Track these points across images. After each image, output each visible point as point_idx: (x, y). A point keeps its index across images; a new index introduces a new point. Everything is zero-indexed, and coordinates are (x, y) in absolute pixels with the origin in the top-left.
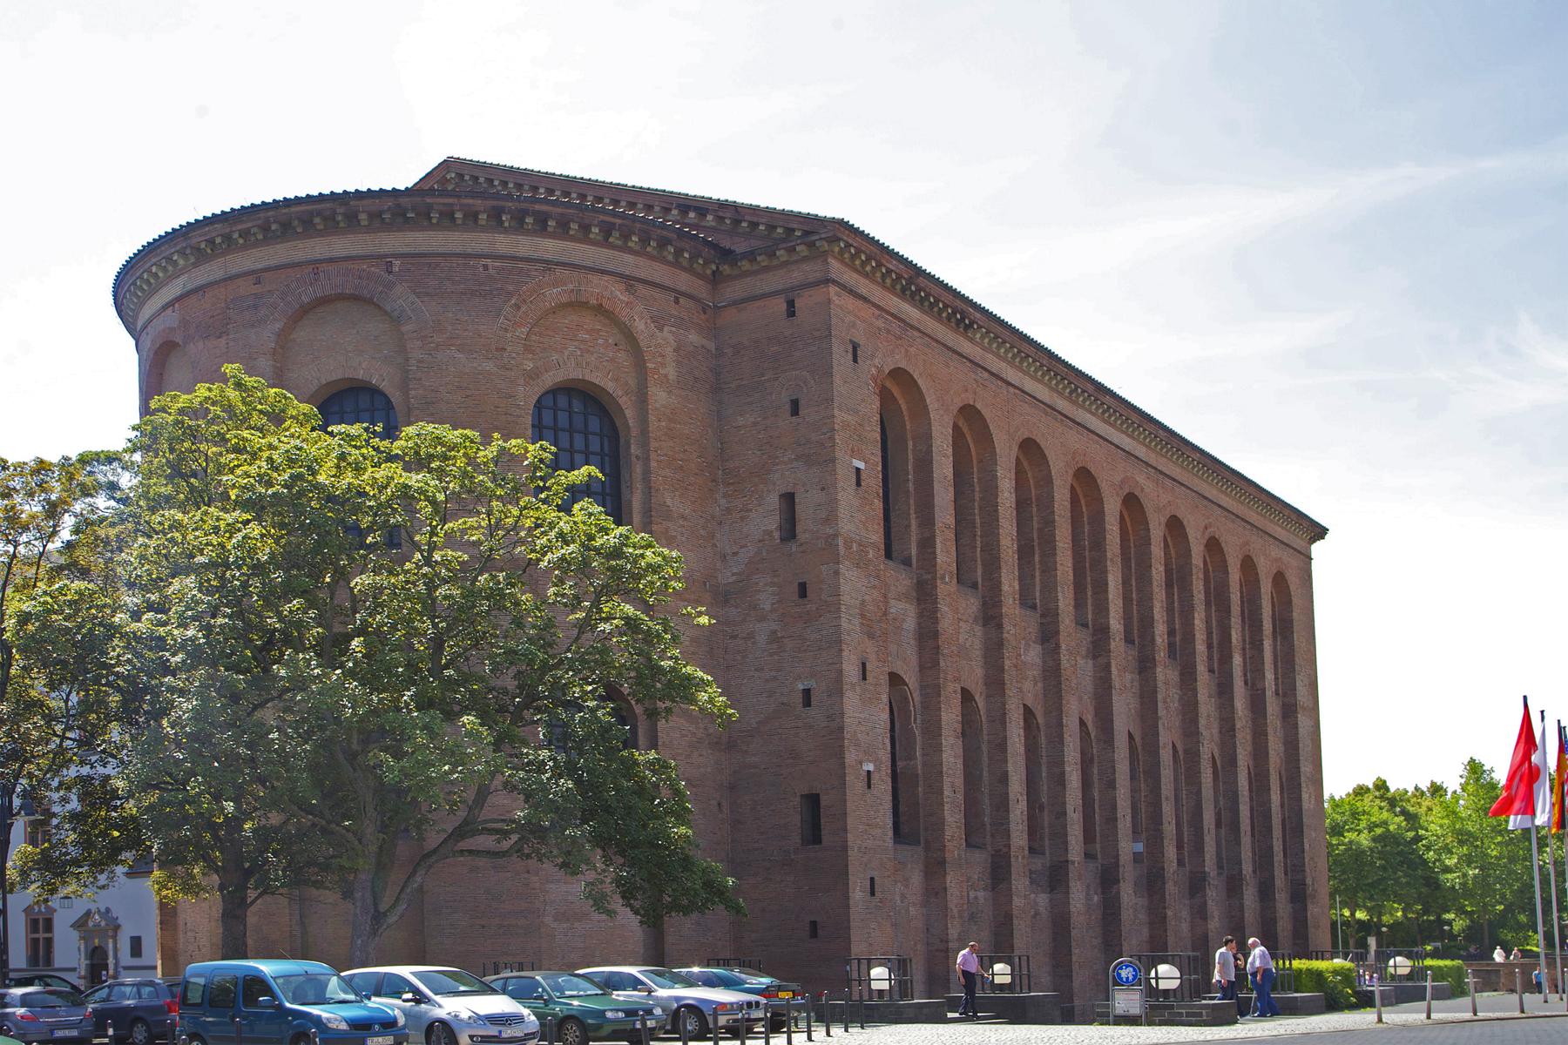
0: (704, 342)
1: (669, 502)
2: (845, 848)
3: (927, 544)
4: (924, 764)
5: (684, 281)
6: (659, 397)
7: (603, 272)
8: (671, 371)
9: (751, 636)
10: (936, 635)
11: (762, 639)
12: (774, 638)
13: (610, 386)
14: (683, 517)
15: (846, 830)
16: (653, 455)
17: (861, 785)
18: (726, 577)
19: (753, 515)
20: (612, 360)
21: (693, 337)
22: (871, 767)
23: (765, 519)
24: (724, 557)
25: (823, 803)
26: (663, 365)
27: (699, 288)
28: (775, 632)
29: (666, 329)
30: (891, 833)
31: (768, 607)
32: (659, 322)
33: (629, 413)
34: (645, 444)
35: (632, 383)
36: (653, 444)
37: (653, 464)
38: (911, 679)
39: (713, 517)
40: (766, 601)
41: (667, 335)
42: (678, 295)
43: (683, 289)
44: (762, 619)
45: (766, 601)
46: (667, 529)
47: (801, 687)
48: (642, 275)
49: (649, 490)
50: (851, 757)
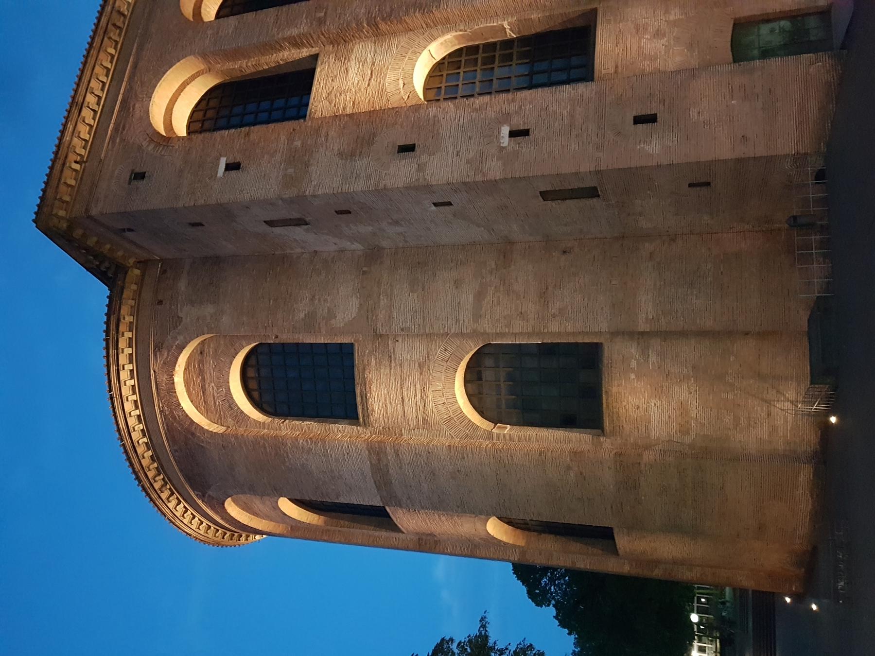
1: (302, 315)
2: (598, 172)
11: (399, 229)
12: (396, 223)
14: (312, 299)
15: (576, 174)
17: (524, 145)
22: (505, 130)
23: (298, 232)
25: (549, 188)
29: (180, 315)
30: (582, 88)
31: (370, 228)
40: (365, 229)
47: (434, 208)
50: (494, 170)
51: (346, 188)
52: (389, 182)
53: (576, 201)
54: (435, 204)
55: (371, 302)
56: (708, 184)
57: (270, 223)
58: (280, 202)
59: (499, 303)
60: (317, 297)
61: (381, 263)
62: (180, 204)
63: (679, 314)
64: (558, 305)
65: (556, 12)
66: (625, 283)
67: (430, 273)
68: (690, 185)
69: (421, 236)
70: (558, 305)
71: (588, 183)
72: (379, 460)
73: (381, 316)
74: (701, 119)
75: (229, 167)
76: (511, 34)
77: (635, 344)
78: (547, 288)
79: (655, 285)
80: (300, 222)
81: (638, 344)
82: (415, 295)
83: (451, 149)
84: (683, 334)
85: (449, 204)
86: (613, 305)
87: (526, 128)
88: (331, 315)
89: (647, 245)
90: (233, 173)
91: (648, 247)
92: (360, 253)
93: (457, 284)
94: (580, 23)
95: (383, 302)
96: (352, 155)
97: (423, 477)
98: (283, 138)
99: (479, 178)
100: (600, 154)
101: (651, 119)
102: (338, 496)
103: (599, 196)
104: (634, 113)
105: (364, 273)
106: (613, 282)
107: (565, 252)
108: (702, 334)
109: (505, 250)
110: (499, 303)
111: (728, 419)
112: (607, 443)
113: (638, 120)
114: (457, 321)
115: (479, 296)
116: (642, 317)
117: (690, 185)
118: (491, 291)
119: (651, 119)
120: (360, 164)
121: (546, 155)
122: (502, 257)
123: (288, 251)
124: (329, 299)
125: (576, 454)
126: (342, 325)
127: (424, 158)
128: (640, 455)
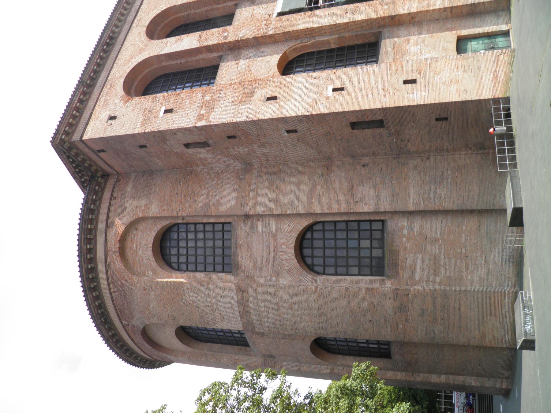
0: (131, 181)
2: (384, 109)
3: (209, 49)
4: (332, 34)
5: (107, 195)
6: (154, 210)
8: (143, 202)
9: (264, 154)
10: (256, 39)
11: (264, 150)
12: (263, 145)
13: (154, 234)
14: (208, 195)
16: (180, 214)
18: (238, 165)
19: (202, 157)
20: (143, 232)
22: (330, 88)
23: (202, 153)
24: (228, 166)
25: (355, 120)
26: (141, 207)
28: (259, 146)
29: (126, 205)
30: (372, 68)
31: (246, 150)
32: (124, 209)
33: (165, 223)
34: (177, 217)
35: (150, 222)
36: (175, 214)
37: (184, 214)
38: (284, 48)
39: (209, 173)
40: (244, 150)
41: (129, 204)
42: (112, 197)
43: (110, 194)
44: (253, 151)
45: (244, 150)
46: (214, 206)
47: (286, 134)
48: (105, 218)
49: (198, 216)
50: (323, 108)
51: (235, 120)
52: (261, 117)
53: (371, 130)
54: (288, 132)
55: (244, 196)
56: (446, 119)
57: (187, 146)
58: (195, 130)
59: (323, 195)
60: (211, 194)
61: (252, 173)
62: (136, 132)
63: (432, 200)
64: (359, 196)
65: (359, 33)
66: (400, 183)
67: (281, 178)
68: (437, 120)
69: (277, 156)
70: (359, 196)
71: (379, 117)
72: (243, 297)
74: (441, 81)
75: (166, 111)
76: (333, 46)
77: (406, 220)
78: (353, 186)
79: (418, 183)
80: (204, 145)
81: (408, 220)
82: (272, 191)
83: (298, 98)
84: (435, 213)
85: (295, 131)
86: (393, 196)
87: (342, 86)
88: (219, 203)
89: (412, 161)
90: (169, 115)
91: (413, 162)
92: (239, 168)
93: (298, 184)
94: (372, 40)
95: (252, 195)
96: (240, 102)
97: (271, 308)
98: (200, 96)
99: (314, 113)
100: (385, 99)
101: (414, 81)
102: (214, 323)
103: (384, 127)
104: (404, 79)
105: (241, 179)
106: (393, 182)
107: (364, 166)
108: (446, 212)
109: (328, 164)
110: (323, 195)
111: (462, 265)
112: (389, 285)
113: (406, 82)
114: (297, 206)
115: (312, 191)
116: (410, 202)
117: (437, 120)
118: (319, 188)
119: (414, 81)
120: (243, 107)
121: (354, 101)
122: (326, 169)
123: (195, 168)
124: (218, 194)
125: (369, 290)
126: (226, 209)
127: (281, 104)
128: (409, 290)
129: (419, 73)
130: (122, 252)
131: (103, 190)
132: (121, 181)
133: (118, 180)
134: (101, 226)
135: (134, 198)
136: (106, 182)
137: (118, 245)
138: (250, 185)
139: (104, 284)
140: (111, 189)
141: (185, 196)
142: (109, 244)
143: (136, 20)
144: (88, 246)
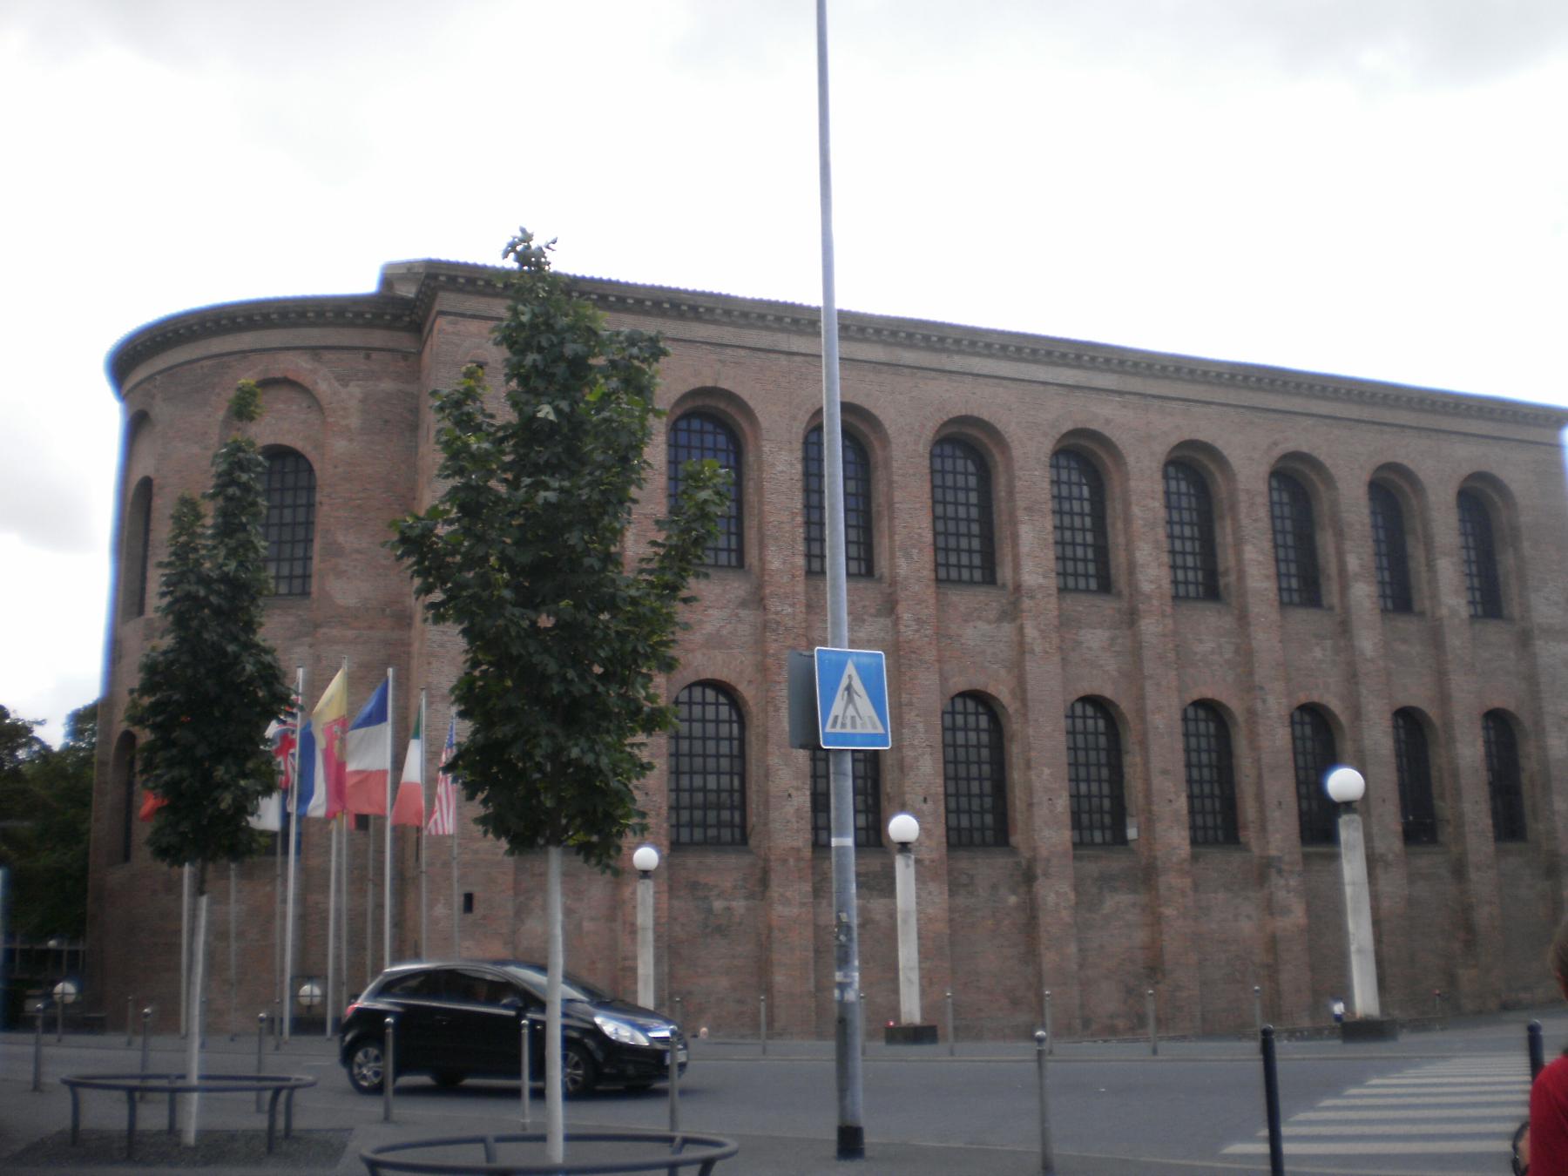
1: (341, 539)
6: (340, 446)
7: (288, 349)
8: (354, 422)
21: (387, 385)
27: (403, 341)
32: (344, 380)
41: (355, 390)
42: (368, 351)
48: (329, 343)
73: (334, 632)
95: (350, 634)
129: (484, 917)
130: (267, 383)
131: (388, 327)
132: (402, 364)
133: (406, 356)
134: (314, 336)
135: (363, 401)
136: (405, 329)
137: (279, 375)
138: (371, 628)
139: (218, 345)
140: (391, 345)
141: (359, 506)
142: (281, 356)
143: (742, 352)
144: (274, 316)
